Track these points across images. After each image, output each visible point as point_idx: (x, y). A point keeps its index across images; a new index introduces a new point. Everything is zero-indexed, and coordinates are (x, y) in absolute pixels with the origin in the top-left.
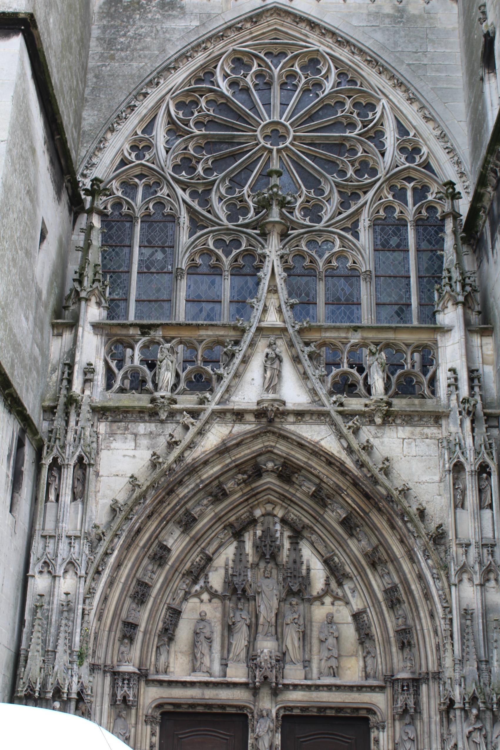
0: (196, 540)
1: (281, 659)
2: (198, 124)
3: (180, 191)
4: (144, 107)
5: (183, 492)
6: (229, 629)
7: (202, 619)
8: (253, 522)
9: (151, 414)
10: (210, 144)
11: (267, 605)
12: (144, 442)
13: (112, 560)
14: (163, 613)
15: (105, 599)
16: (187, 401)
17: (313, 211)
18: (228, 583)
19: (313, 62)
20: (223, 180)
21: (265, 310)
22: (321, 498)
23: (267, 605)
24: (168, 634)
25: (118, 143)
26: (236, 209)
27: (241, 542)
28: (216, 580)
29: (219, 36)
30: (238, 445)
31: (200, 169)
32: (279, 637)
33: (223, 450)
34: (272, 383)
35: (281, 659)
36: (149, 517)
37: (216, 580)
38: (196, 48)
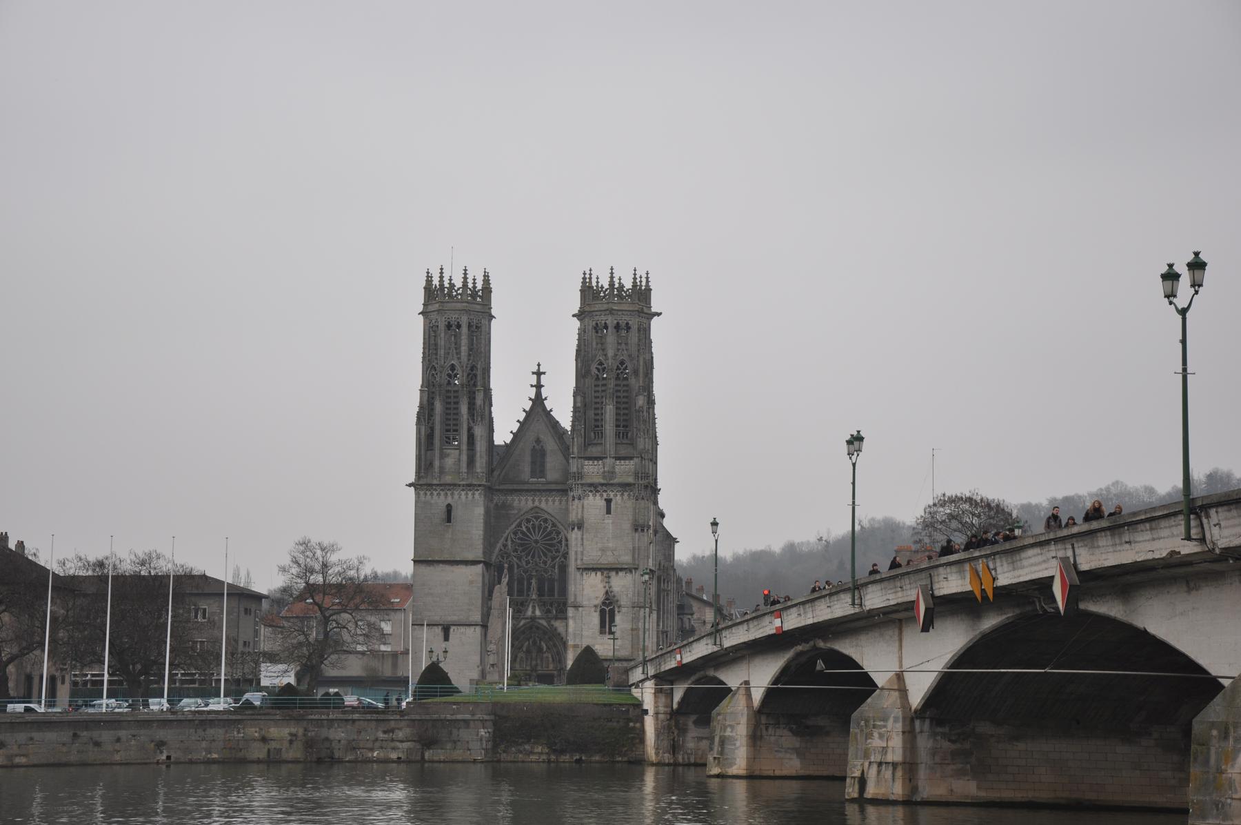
10: (521, 545)
11: (534, 655)
17: (545, 563)
19: (546, 521)
22: (545, 633)
23: (534, 655)
25: (499, 545)
26: (528, 563)
34: (533, 612)
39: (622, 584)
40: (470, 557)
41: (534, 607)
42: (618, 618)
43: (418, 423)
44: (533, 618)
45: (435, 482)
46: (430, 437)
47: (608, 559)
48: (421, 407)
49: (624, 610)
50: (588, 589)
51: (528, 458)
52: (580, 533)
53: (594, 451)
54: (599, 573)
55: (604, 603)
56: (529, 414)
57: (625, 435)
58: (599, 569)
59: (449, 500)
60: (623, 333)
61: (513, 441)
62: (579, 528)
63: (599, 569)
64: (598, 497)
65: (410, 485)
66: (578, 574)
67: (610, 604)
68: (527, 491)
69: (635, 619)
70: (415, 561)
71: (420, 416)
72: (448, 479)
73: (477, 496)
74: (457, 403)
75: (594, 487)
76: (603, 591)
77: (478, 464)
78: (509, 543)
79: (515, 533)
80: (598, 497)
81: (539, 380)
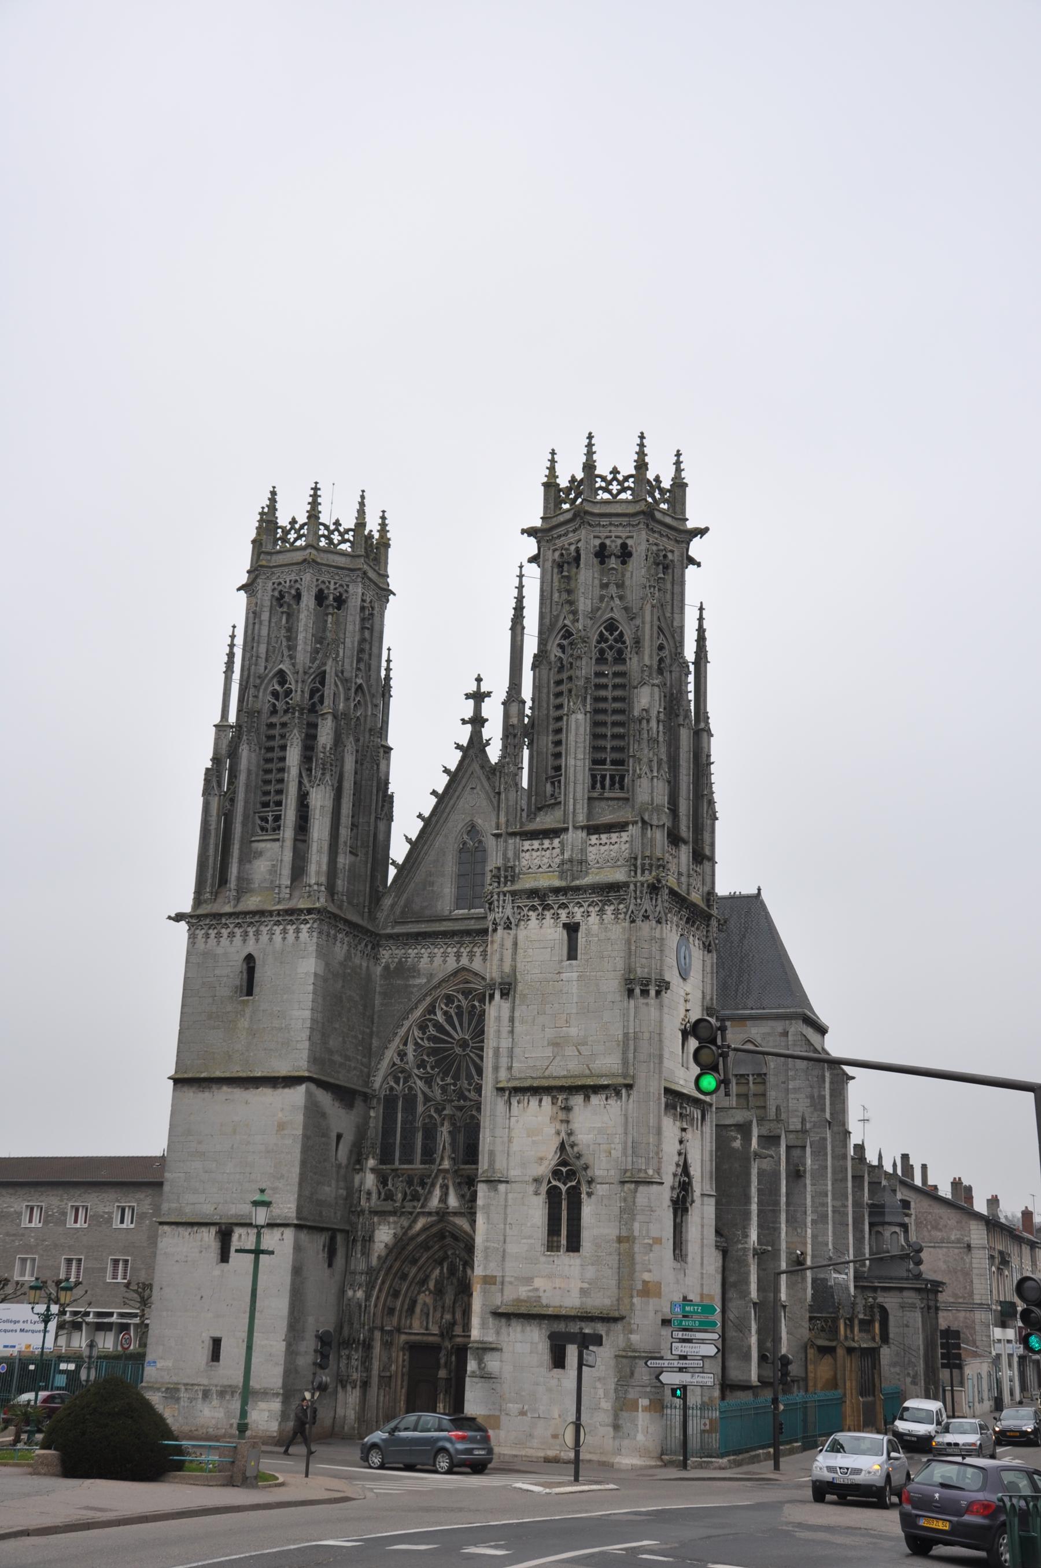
0: (420, 1269)
1: (453, 1324)
2: (429, 1039)
3: (418, 1082)
4: (402, 1032)
5: (410, 1248)
6: (435, 1308)
7: (425, 1304)
8: (446, 1257)
9: (393, 1213)
10: (433, 1052)
11: (449, 1299)
12: (392, 1226)
13: (379, 1281)
14: (407, 1301)
15: (378, 1298)
16: (409, 1206)
18: (435, 1286)
20: (438, 1074)
21: (442, 1159)
23: (449, 1299)
24: (411, 1310)
25: (391, 1053)
26: (444, 1089)
27: (442, 1268)
28: (431, 1285)
29: (435, 988)
30: (431, 1226)
31: (428, 1068)
32: (454, 1314)
33: (424, 1229)
34: (444, 1199)
35: (453, 1324)
36: (395, 1260)
37: (431, 1285)
38: (426, 995)
39: (595, 1123)
40: (283, 1069)
41: (445, 1188)
42: (588, 1211)
43: (207, 792)
44: (442, 1214)
45: (228, 909)
46: (228, 816)
47: (567, 1066)
48: (216, 759)
49: (600, 1190)
50: (521, 1139)
51: (450, 866)
52: (506, 1006)
53: (546, 820)
54: (547, 1100)
55: (556, 1173)
56: (455, 777)
57: (619, 781)
58: (547, 1090)
59: (251, 947)
60: (613, 562)
61: (423, 832)
62: (505, 994)
63: (547, 1090)
64: (549, 921)
65: (178, 917)
66: (501, 1104)
67: (571, 1174)
68: (445, 934)
69: (628, 1212)
70: (178, 1082)
71: (212, 777)
72: (252, 902)
73: (304, 935)
74: (283, 748)
75: (540, 899)
76: (555, 1143)
77: (312, 868)
78: (410, 1049)
79: (423, 1028)
80: (549, 921)
81: (478, 709)
